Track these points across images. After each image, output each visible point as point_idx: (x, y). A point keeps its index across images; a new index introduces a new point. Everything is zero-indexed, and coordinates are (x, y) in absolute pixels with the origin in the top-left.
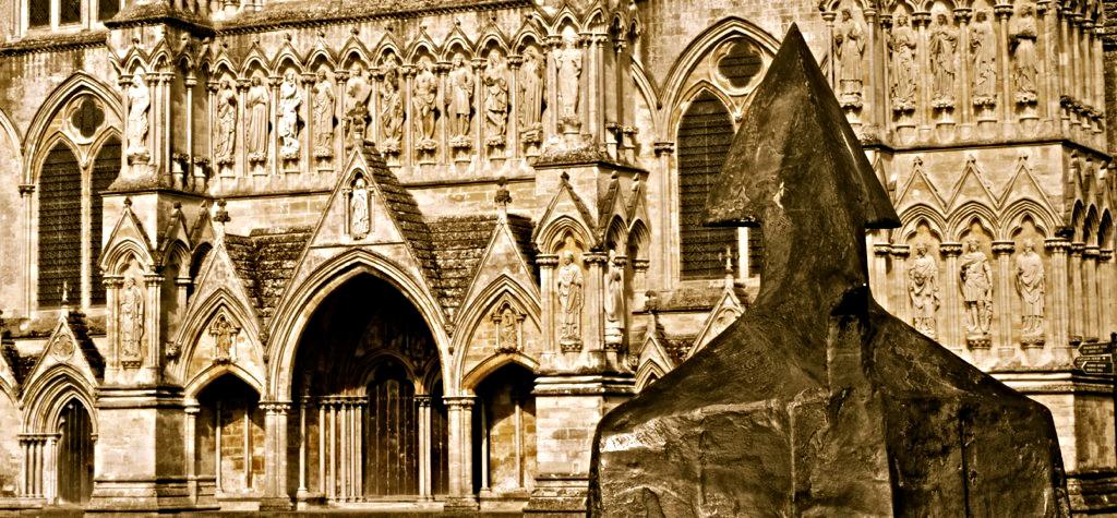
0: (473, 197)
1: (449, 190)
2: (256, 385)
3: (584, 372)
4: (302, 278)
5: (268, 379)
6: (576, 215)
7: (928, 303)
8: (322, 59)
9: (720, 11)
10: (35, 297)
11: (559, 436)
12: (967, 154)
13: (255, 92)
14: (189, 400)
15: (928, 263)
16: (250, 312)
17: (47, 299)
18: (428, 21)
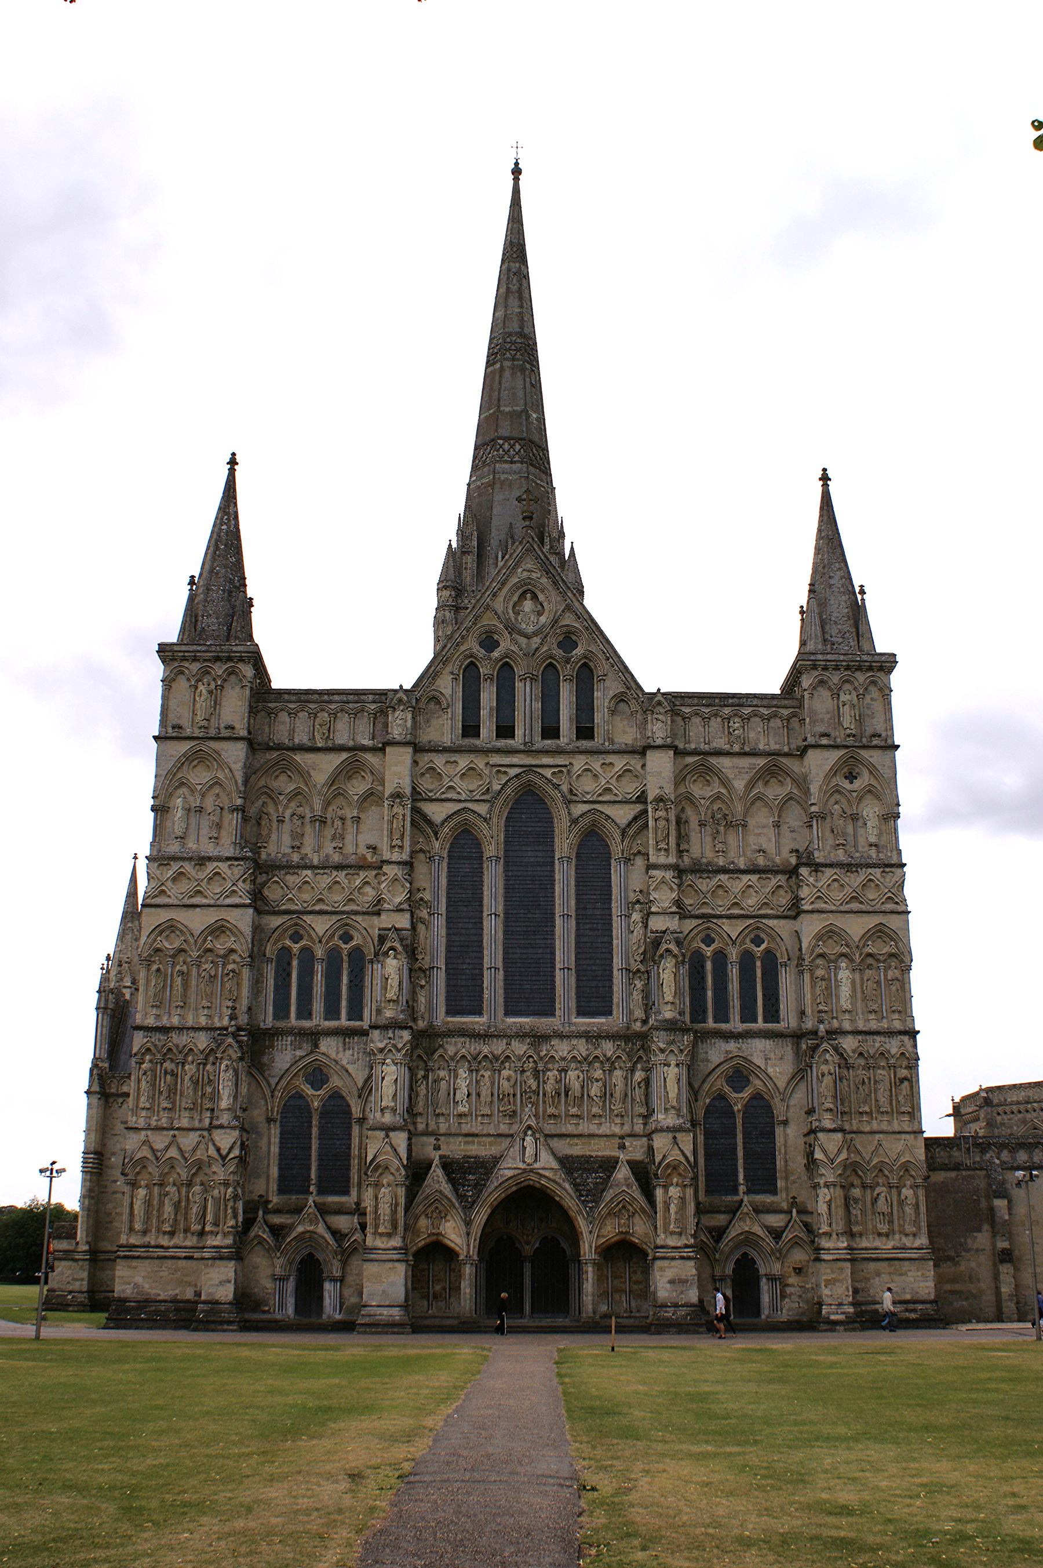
0: (583, 1144)
1: (568, 1139)
2: (457, 1249)
4: (493, 1187)
5: (468, 1245)
6: (683, 1159)
7: (859, 1212)
8: (486, 1056)
9: (730, 1052)
11: (671, 1282)
12: (877, 1136)
15: (856, 1192)
16: (457, 1205)
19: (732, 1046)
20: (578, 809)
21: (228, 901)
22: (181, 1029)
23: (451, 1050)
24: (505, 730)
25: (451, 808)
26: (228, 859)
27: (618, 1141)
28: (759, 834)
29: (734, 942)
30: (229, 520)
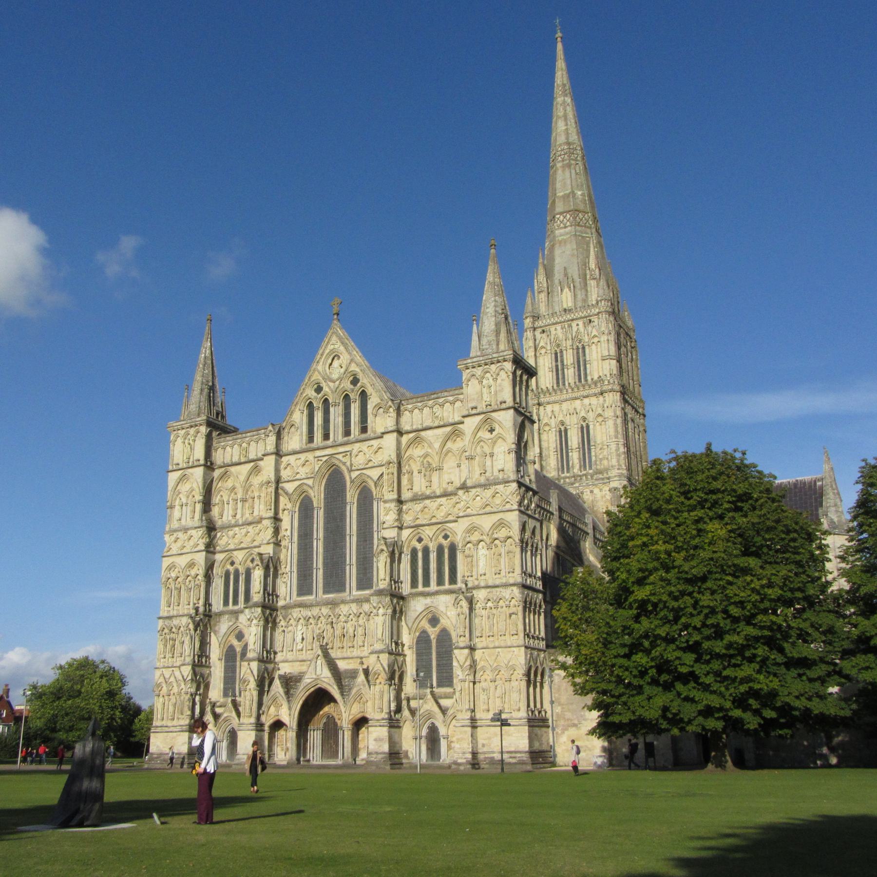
1: (347, 661)
3: (383, 719)
4: (301, 689)
6: (382, 669)
10: (222, 694)
11: (375, 740)
13: (290, 628)
14: (266, 728)
17: (225, 695)
18: (342, 606)
19: (428, 601)
20: (354, 475)
21: (196, 549)
22: (176, 616)
23: (295, 615)
24: (326, 436)
25: (297, 483)
26: (196, 528)
27: (359, 660)
28: (450, 473)
29: (431, 540)
30: (206, 351)
